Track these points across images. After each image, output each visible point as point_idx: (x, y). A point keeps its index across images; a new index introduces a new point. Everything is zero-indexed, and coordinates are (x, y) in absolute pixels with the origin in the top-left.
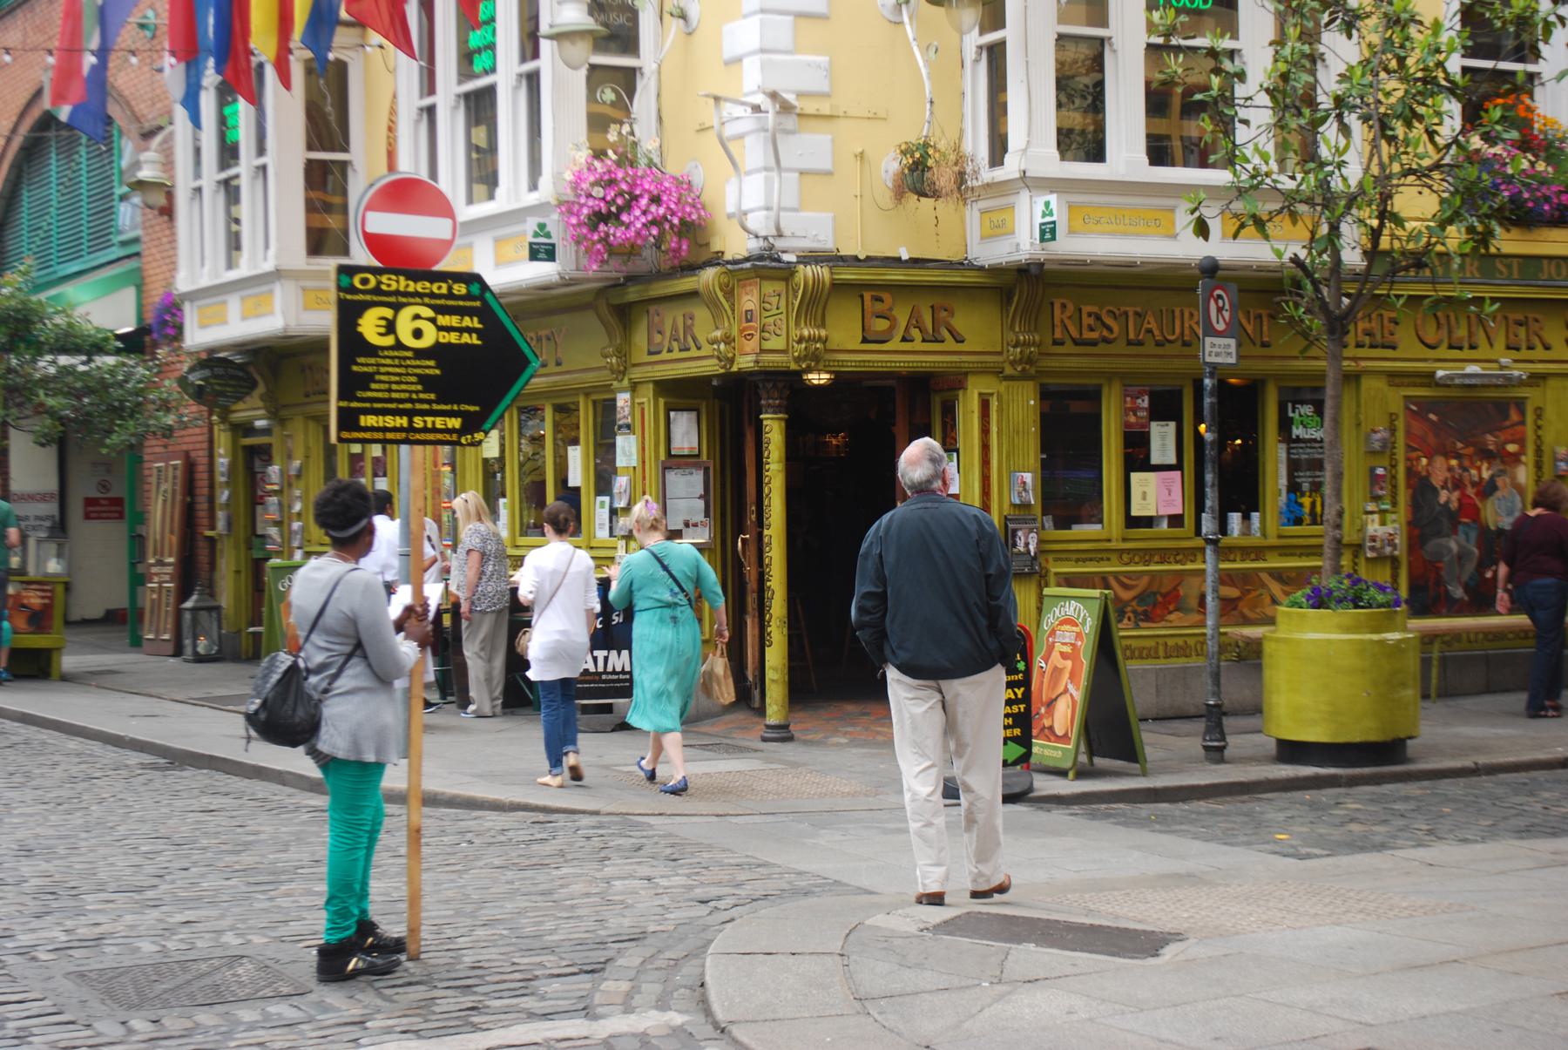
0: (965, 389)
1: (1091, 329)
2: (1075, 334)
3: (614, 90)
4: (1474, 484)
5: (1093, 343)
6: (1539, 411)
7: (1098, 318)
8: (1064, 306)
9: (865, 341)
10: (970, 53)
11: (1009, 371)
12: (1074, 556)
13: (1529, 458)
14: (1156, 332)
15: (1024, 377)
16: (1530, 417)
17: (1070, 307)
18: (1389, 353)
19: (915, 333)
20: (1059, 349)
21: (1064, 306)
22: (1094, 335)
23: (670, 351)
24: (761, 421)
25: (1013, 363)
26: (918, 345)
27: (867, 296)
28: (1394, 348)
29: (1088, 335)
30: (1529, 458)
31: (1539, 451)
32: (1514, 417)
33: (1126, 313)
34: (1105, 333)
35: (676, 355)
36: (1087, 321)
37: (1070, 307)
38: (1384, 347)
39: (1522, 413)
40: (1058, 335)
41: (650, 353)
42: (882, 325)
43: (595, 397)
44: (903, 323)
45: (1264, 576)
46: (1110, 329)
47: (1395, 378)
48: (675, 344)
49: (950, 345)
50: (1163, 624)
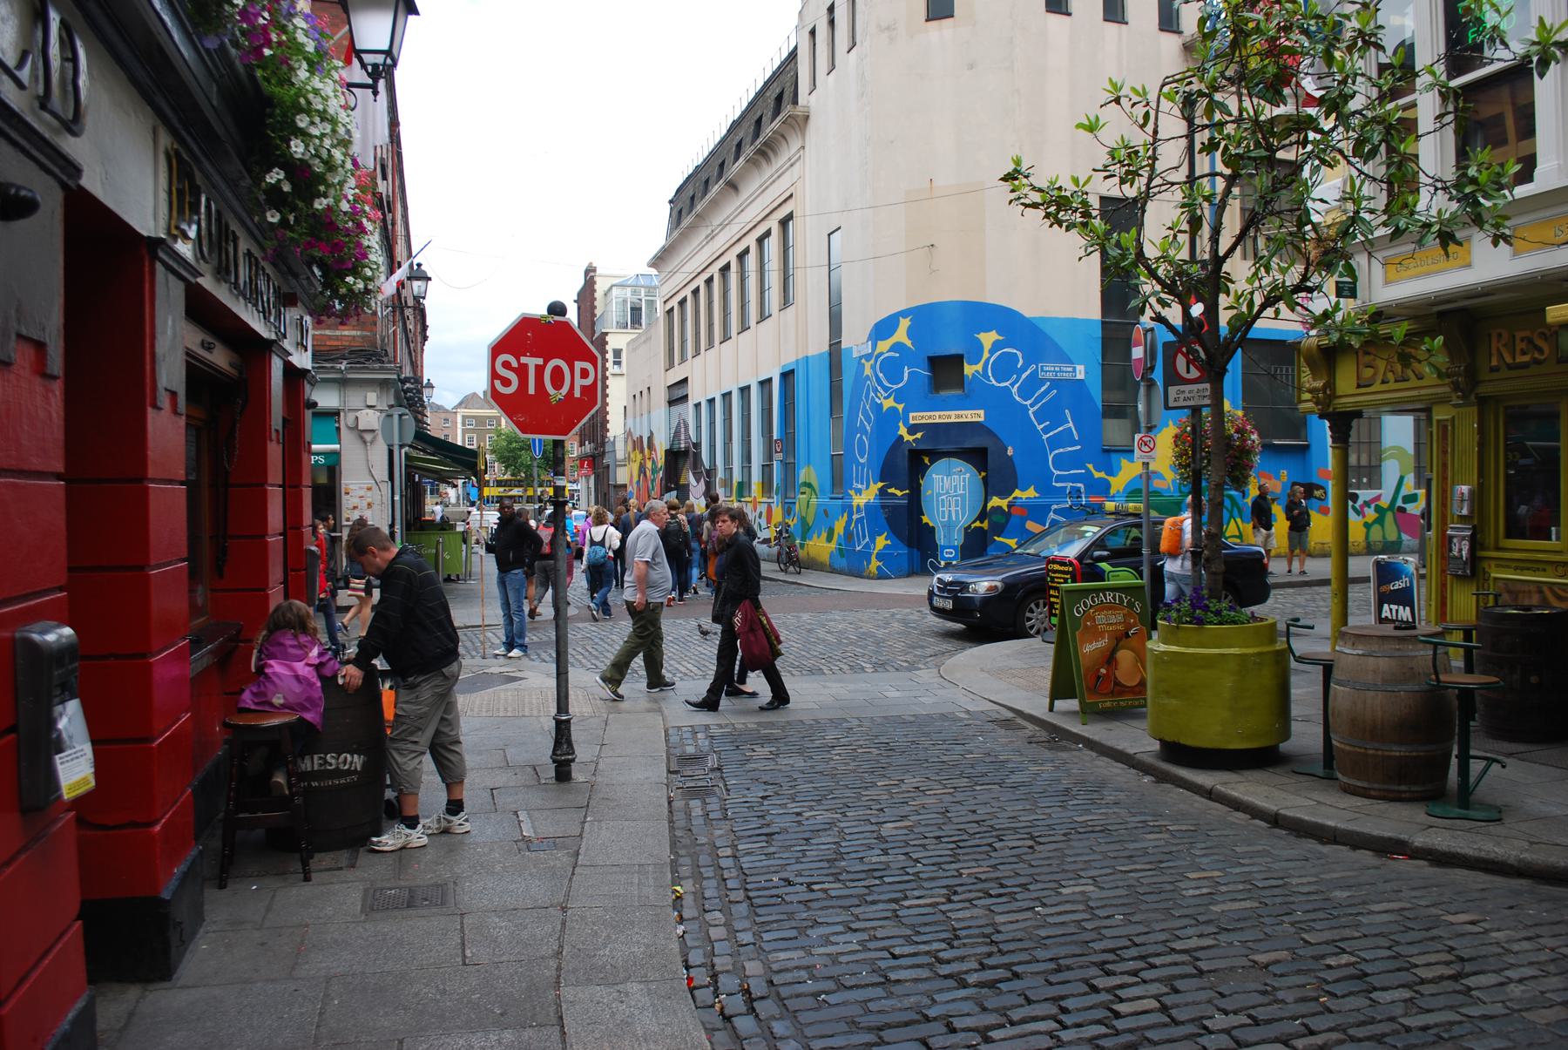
1: (1524, 353)
5: (1525, 366)
7: (1530, 341)
8: (1500, 335)
9: (1359, 386)
12: (1513, 564)
19: (1390, 376)
20: (1495, 376)
21: (1500, 335)
22: (1526, 358)
26: (1392, 385)
29: (1521, 359)
34: (1536, 355)
36: (1520, 346)
37: (1505, 335)
40: (1494, 362)
42: (1368, 373)
44: (1382, 370)
46: (1541, 351)
49: (1414, 382)
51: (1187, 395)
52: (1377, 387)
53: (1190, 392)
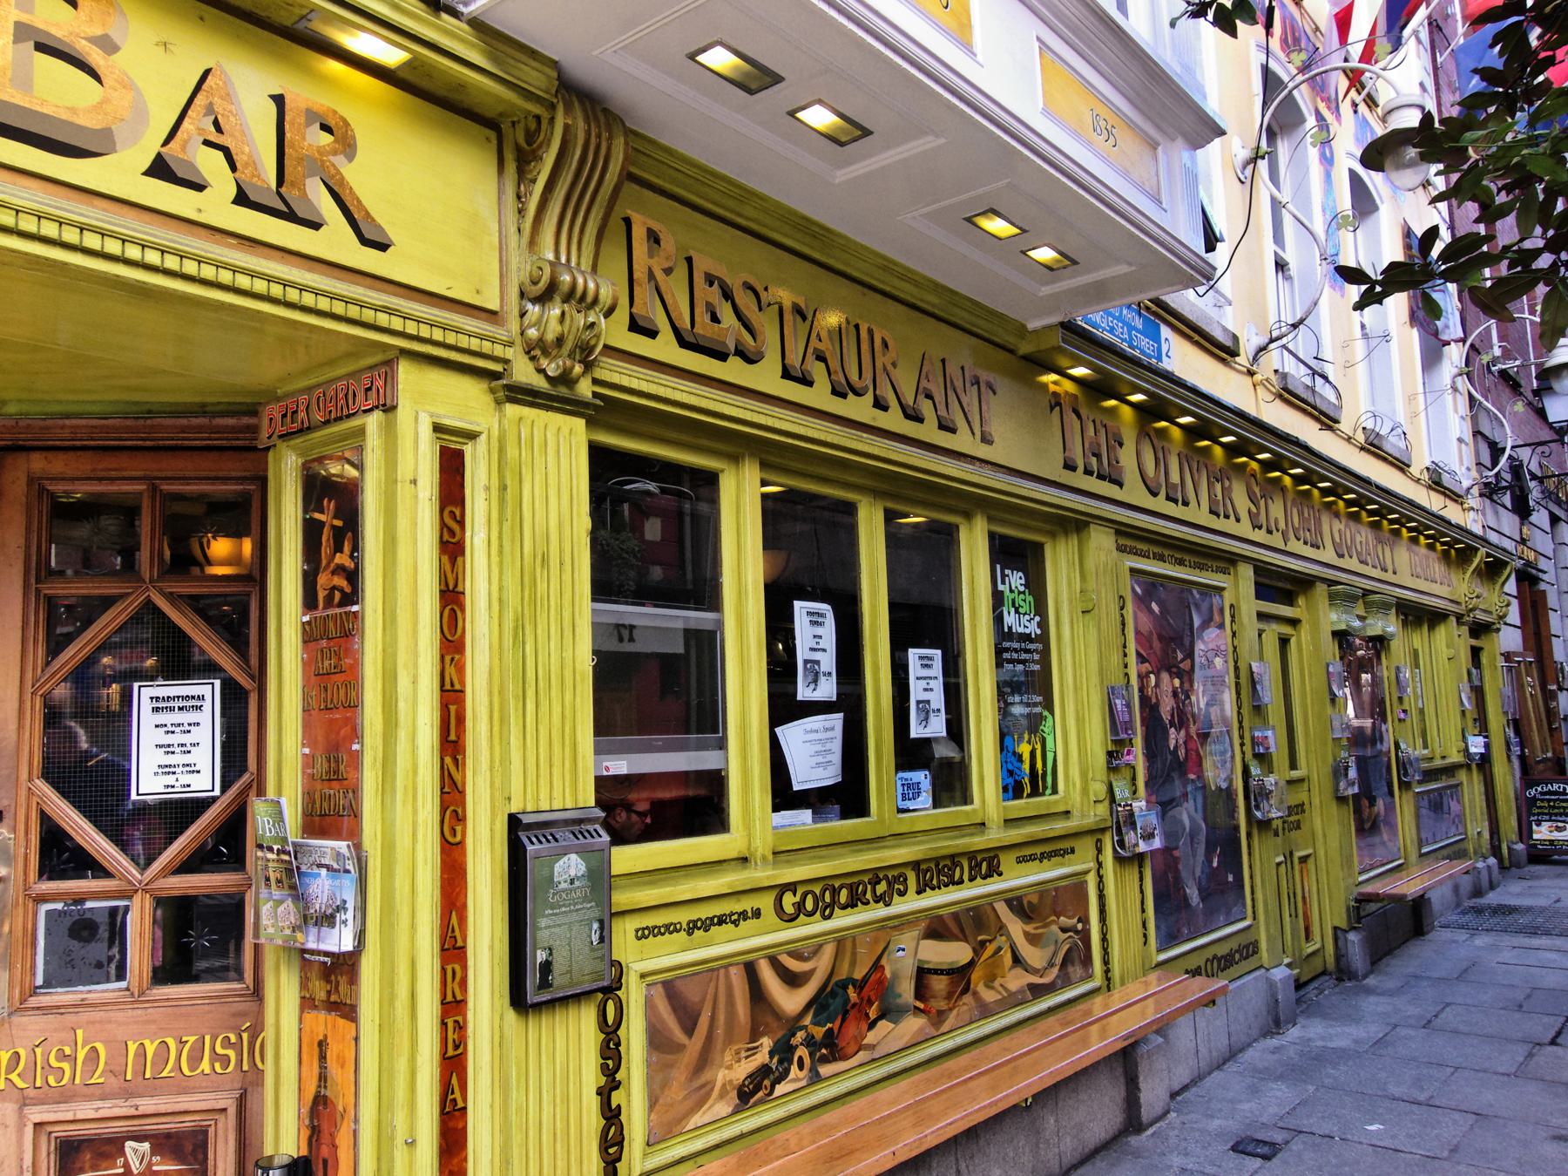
0: (389, 409)
7: (727, 295)
8: (654, 238)
11: (524, 372)
14: (834, 364)
25: (536, 349)
28: (1121, 485)
29: (704, 327)
45: (1001, 908)
49: (337, 241)
50: (862, 1056)
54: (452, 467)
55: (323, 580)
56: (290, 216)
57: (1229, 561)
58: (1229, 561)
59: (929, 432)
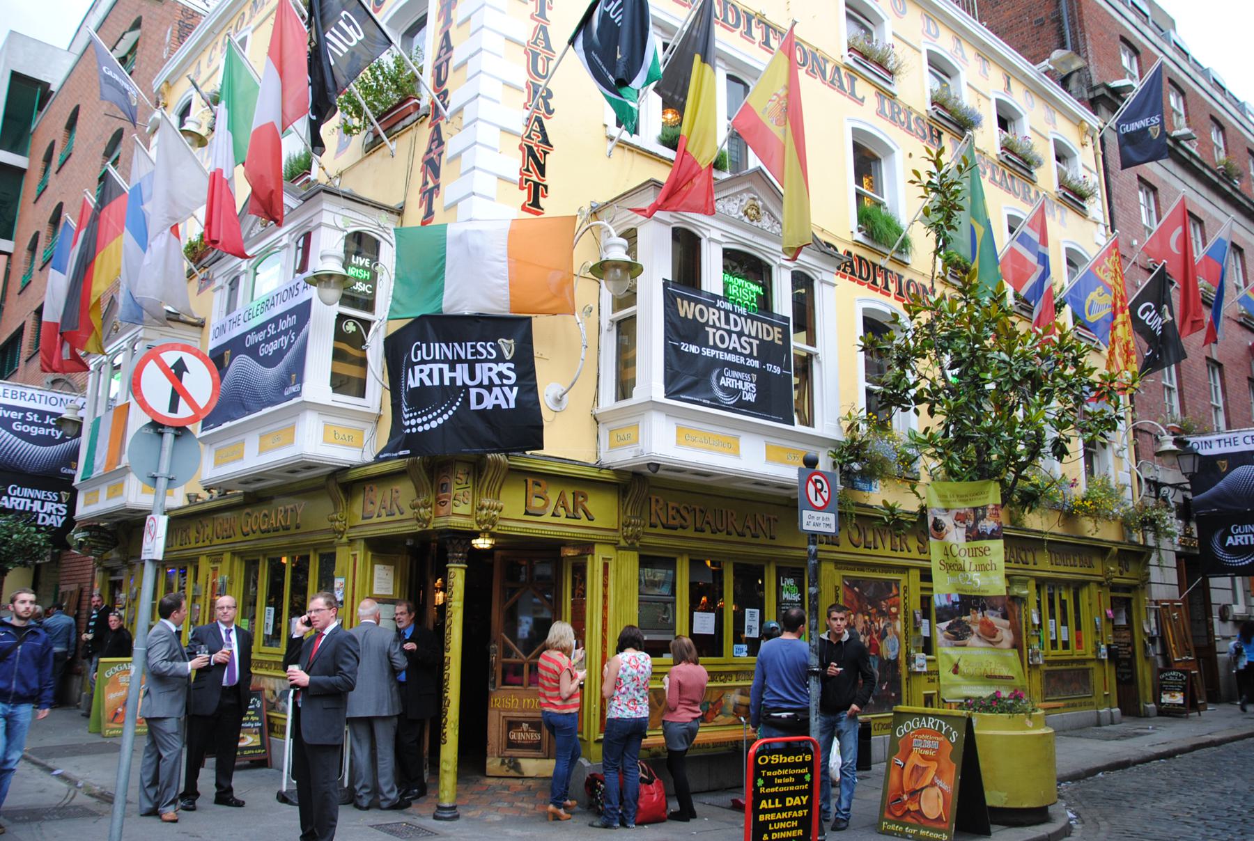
0: (593, 554)
2: (664, 521)
3: (355, 324)
4: (877, 632)
6: (906, 589)
7: (678, 511)
8: (657, 501)
9: (527, 513)
10: (605, 324)
11: (623, 543)
13: (901, 616)
14: (713, 524)
15: (631, 548)
16: (902, 591)
17: (661, 502)
18: (835, 548)
19: (561, 511)
21: (657, 501)
23: (379, 516)
24: (447, 569)
25: (625, 538)
26: (563, 520)
27: (530, 481)
29: (671, 522)
30: (901, 616)
31: (905, 612)
32: (894, 591)
33: (695, 510)
34: (683, 522)
35: (384, 518)
37: (661, 502)
38: (833, 544)
39: (898, 588)
41: (364, 518)
42: (538, 503)
43: (321, 551)
46: (684, 519)
47: (839, 564)
48: (383, 512)
49: (584, 521)
50: (712, 724)
51: (815, 520)
52: (547, 518)
53: (818, 518)
54: (606, 567)
55: (577, 591)
56: (575, 518)
57: (904, 569)
58: (904, 569)
59: (748, 539)
